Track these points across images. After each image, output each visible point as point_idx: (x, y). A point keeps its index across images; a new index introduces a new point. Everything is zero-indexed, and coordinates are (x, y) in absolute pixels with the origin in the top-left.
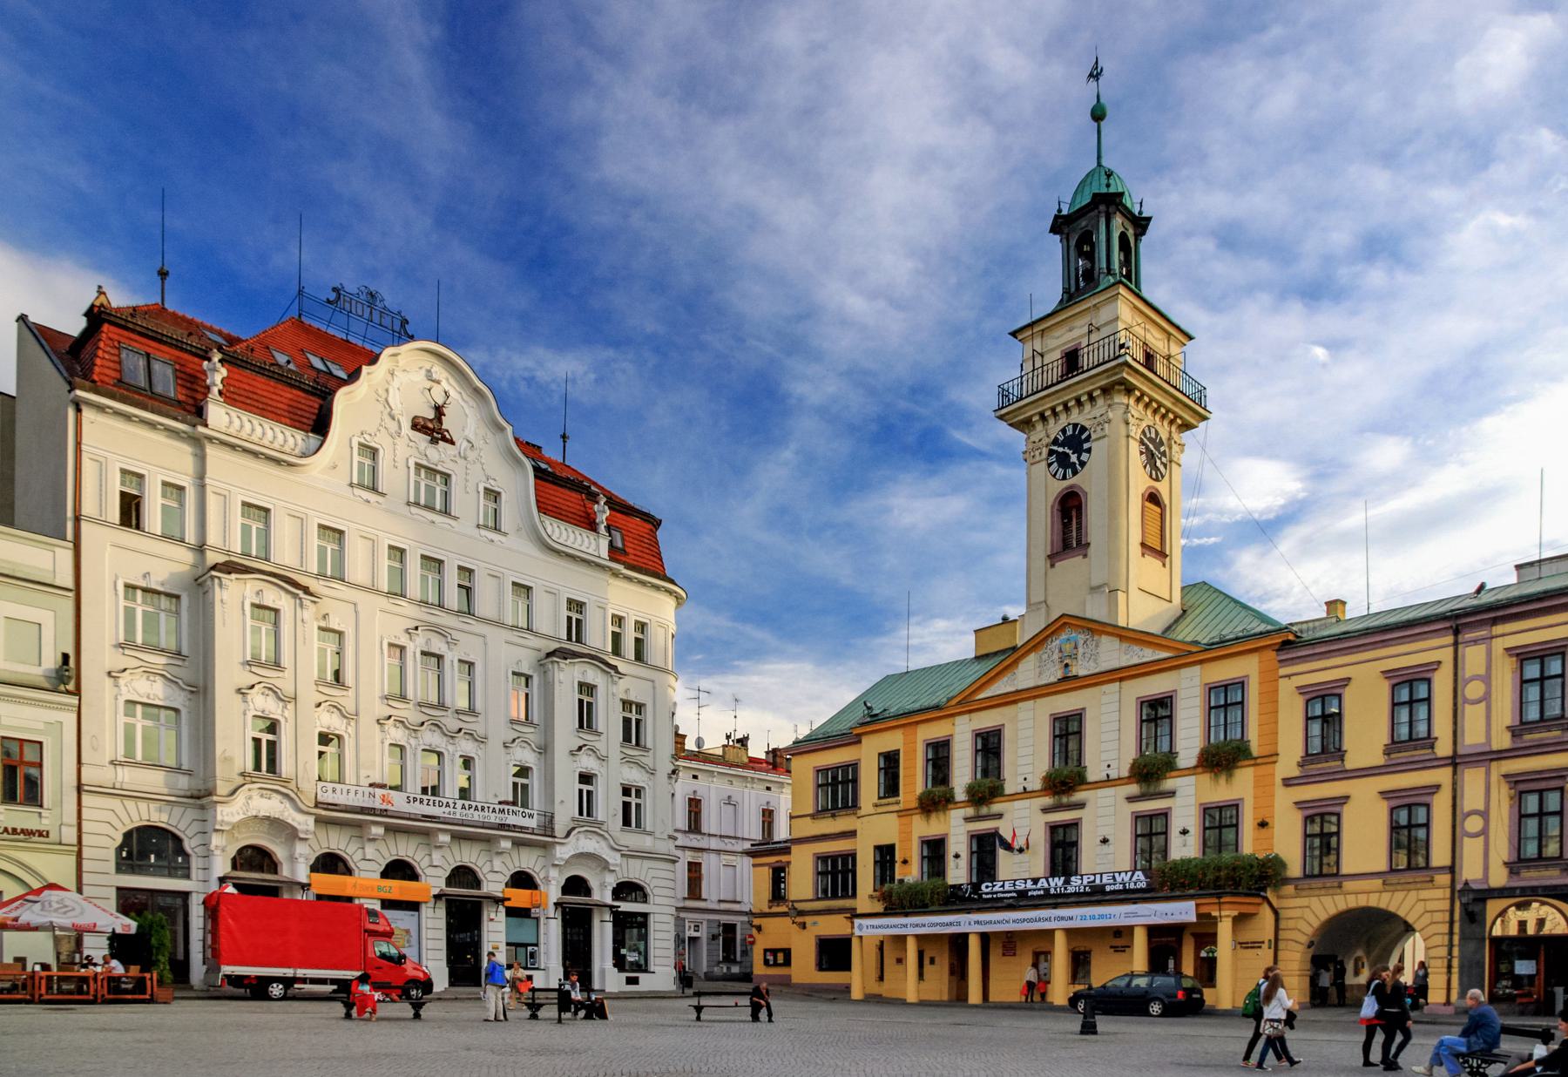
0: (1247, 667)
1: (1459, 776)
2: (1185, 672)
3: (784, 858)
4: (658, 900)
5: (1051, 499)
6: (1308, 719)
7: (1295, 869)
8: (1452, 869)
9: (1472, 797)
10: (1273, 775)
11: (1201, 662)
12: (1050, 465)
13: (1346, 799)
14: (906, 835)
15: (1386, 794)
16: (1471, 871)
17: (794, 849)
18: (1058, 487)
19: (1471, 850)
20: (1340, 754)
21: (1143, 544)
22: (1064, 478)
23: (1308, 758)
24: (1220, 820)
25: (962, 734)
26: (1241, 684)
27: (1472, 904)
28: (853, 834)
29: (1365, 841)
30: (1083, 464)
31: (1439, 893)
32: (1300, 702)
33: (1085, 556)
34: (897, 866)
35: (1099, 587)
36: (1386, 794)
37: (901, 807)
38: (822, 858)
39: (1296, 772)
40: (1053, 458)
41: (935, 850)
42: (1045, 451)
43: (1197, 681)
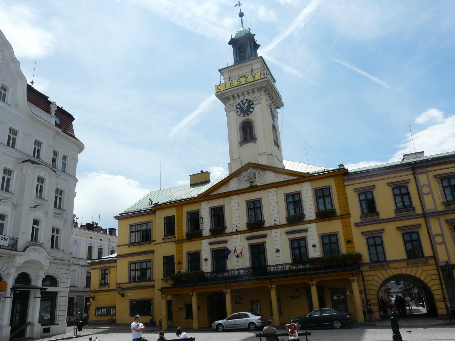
0: (331, 183)
1: (427, 221)
2: (304, 184)
3: (108, 265)
4: (63, 285)
7: (366, 258)
8: (435, 257)
11: (310, 180)
12: (237, 112)
13: (382, 231)
14: (180, 252)
15: (399, 228)
17: (119, 261)
18: (241, 119)
21: (274, 141)
22: (244, 116)
23: (363, 215)
24: (329, 241)
25: (205, 211)
28: (152, 252)
29: (395, 248)
30: (251, 112)
31: (431, 267)
33: (255, 143)
34: (176, 265)
35: (263, 153)
36: (399, 228)
39: (359, 220)
40: (238, 110)
41: (195, 258)
42: (235, 108)
43: (309, 187)
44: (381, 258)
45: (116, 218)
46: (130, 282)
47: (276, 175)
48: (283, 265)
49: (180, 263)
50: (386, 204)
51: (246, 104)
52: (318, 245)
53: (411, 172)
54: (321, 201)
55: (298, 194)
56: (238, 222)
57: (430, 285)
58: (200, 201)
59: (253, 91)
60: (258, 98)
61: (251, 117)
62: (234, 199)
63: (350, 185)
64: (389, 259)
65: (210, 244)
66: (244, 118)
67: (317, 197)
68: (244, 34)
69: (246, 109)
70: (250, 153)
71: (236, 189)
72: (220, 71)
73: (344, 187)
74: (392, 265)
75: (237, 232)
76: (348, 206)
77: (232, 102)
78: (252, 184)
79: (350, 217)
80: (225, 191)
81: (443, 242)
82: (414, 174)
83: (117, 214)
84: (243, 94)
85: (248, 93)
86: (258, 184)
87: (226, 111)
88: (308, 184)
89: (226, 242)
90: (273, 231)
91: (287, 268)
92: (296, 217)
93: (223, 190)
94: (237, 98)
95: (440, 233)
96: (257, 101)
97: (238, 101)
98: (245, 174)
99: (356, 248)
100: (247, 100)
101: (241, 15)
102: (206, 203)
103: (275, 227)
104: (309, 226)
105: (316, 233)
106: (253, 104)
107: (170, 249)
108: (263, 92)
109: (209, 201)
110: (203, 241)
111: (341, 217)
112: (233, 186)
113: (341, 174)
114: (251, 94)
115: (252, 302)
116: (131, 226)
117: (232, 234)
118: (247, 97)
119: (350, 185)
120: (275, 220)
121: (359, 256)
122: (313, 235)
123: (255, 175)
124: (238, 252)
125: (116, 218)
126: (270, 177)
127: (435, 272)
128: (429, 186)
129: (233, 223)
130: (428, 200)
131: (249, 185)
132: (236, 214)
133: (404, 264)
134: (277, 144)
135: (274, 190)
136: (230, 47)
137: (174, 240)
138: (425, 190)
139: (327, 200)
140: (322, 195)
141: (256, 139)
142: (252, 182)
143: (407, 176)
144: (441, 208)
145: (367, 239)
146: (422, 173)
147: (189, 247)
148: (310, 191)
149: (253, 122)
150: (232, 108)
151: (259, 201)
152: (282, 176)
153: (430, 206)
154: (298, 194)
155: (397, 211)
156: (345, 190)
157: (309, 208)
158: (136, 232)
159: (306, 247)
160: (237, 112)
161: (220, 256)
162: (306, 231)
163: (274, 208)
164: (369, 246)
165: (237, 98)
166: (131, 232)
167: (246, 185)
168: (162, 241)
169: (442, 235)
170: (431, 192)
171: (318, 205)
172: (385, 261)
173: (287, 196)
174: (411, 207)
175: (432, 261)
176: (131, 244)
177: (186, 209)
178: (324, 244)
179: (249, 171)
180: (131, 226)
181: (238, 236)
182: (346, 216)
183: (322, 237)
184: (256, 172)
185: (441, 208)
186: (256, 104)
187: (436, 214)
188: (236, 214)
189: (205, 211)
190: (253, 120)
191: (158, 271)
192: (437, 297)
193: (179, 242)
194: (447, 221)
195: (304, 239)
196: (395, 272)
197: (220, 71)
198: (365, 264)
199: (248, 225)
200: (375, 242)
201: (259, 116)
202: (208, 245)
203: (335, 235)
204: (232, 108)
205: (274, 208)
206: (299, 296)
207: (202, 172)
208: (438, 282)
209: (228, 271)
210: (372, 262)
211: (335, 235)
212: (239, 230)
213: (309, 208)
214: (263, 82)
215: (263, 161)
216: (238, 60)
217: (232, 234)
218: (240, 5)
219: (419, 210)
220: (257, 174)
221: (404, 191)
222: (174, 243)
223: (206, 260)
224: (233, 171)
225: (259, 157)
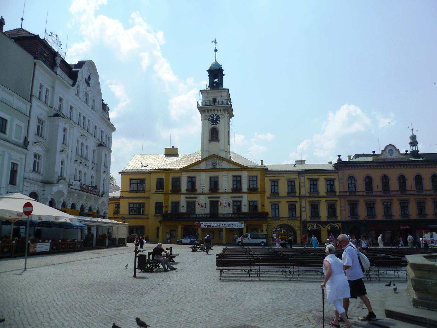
2: (244, 172)
6: (271, 186)
7: (270, 215)
8: (300, 217)
9: (303, 204)
10: (265, 196)
13: (280, 202)
15: (287, 202)
16: (304, 218)
19: (304, 214)
20: (278, 193)
23: (272, 193)
26: (256, 176)
27: (304, 224)
28: (148, 198)
29: (284, 211)
30: (218, 123)
31: (298, 222)
36: (287, 202)
37: (164, 192)
38: (130, 203)
39: (269, 196)
41: (176, 205)
43: (246, 174)
44: (277, 215)
45: (120, 173)
46: (130, 215)
48: (228, 214)
49: (166, 207)
50: (283, 189)
51: (215, 117)
52: (247, 206)
53: (298, 175)
54: (251, 182)
55: (240, 177)
56: (204, 187)
57: (296, 230)
59: (220, 110)
61: (217, 126)
62: (203, 174)
64: (280, 216)
65: (186, 198)
66: (213, 126)
68: (218, 68)
69: (214, 120)
70: (215, 148)
72: (201, 91)
74: (281, 219)
75: (203, 193)
76: (264, 187)
77: (206, 113)
80: (198, 168)
81: (305, 211)
82: (299, 176)
83: (121, 171)
84: (214, 110)
85: (217, 110)
86: (218, 168)
88: (246, 172)
90: (224, 195)
91: (230, 216)
92: (237, 189)
94: (210, 112)
95: (305, 206)
97: (211, 114)
98: (211, 160)
100: (216, 115)
101: (216, 51)
103: (225, 193)
104: (244, 195)
105: (247, 199)
106: (219, 118)
107: (160, 198)
108: (226, 112)
111: (261, 193)
112: (203, 166)
113: (264, 170)
114: (219, 111)
116: (131, 180)
117: (200, 194)
118: (216, 113)
121: (267, 214)
122: (245, 200)
124: (203, 205)
125: (120, 173)
126: (225, 165)
127: (299, 224)
128: (304, 183)
129: (201, 188)
130: (303, 190)
131: (212, 167)
132: (203, 182)
133: (287, 219)
134: (229, 144)
136: (207, 74)
137: (163, 193)
138: (302, 185)
139: (255, 182)
140: (252, 179)
143: (295, 176)
144: (307, 194)
145: (272, 205)
146: (302, 176)
147: (173, 198)
152: (232, 165)
153: (303, 193)
154: (240, 177)
155: (288, 193)
156: (264, 179)
157: (245, 186)
158: (134, 184)
161: (191, 205)
162: (242, 197)
163: (225, 182)
164: (272, 209)
165: (210, 112)
166: (131, 184)
167: (210, 167)
168: (154, 192)
169: (305, 207)
170: (305, 186)
171: (249, 184)
172: (279, 217)
173: (233, 177)
174: (295, 192)
175: (299, 219)
176: (130, 191)
177: (172, 175)
178: (250, 206)
179: (213, 159)
180: (131, 180)
182: (263, 192)
183: (250, 201)
184: (218, 160)
185: (307, 194)
187: (305, 197)
188: (203, 182)
190: (219, 128)
191: (151, 209)
192: (298, 235)
193: (166, 194)
194: (309, 201)
195: (240, 202)
196: (282, 223)
197: (201, 91)
199: (210, 190)
200: (275, 206)
201: (221, 126)
202: (185, 198)
203: (257, 201)
205: (225, 182)
207: (173, 147)
208: (300, 228)
209: (196, 214)
210: (272, 217)
211: (257, 201)
212: (204, 192)
213: (245, 186)
215: (222, 155)
217: (200, 194)
218: (216, 43)
219: (298, 195)
220: (217, 162)
221: (293, 184)
222: (163, 195)
223: (183, 207)
224: (204, 157)
225: (220, 152)
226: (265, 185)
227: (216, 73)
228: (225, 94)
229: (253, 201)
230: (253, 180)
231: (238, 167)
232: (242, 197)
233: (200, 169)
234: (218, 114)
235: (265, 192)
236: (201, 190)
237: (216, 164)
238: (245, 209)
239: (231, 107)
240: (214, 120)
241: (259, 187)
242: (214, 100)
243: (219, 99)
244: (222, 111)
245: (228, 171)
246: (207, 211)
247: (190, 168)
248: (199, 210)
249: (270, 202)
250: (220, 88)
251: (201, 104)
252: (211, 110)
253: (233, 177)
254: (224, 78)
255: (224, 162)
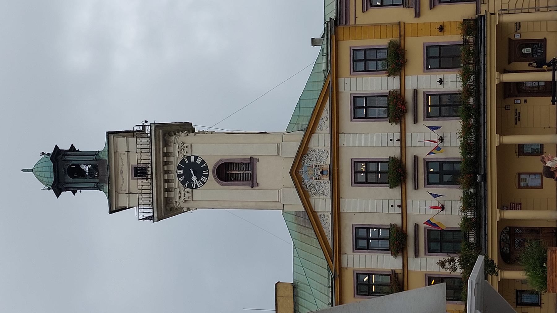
5: (218, 185)
11: (337, 77)
30: (203, 162)
32: (373, 11)
33: (257, 160)
39: (412, 11)
47: (318, 131)
52: (440, 76)
55: (355, 98)
58: (340, 268)
60: (181, 148)
61: (211, 164)
63: (356, 18)
65: (417, 255)
67: (366, 70)
71: (329, 201)
72: (111, 212)
73: (356, 26)
76: (387, 25)
77: (175, 195)
78: (325, 173)
79: (404, 23)
80: (329, 221)
84: (166, 172)
86: (328, 162)
87: (189, 209)
89: (417, 226)
90: (408, 144)
93: (327, 224)
94: (172, 185)
96: (186, 149)
97: (177, 183)
98: (307, 182)
99: (452, 20)
100: (179, 168)
102: (344, 257)
103: (402, 140)
106: (189, 158)
108: (173, 138)
109: (342, 251)
110: (411, 268)
111: (402, 36)
112: (323, 205)
115: (520, 187)
119: (356, 18)
120: (391, 140)
123: (312, 167)
126: (321, 141)
132: (372, 205)
135: (341, 136)
136: (66, 195)
140: (363, 61)
141: (252, 158)
142: (322, 173)
148: (354, 79)
149: (221, 160)
150: (187, 195)
151: (355, 163)
154: (355, 98)
156: (362, 26)
157: (381, 84)
159: (440, 95)
160: (197, 187)
162: (416, 92)
163: (372, 140)
165: (172, 185)
167: (326, 184)
179: (303, 176)
181: (409, 203)
183: (428, 67)
184: (307, 163)
186: (191, 152)
188: (372, 205)
189: (357, 261)
197: (111, 212)
198: (478, 10)
201: (211, 154)
202: (417, 260)
203: (428, 48)
204: (187, 195)
205: (372, 140)
206: (516, 110)
211: (428, 48)
213: (381, 84)
214: (155, 134)
216: (97, 180)
217: (404, 215)
226: (380, 25)
227: (68, 170)
228: (122, 142)
229: (428, 58)
230: (366, 60)
231: (328, 103)
232: (416, 92)
233: (333, 213)
234: (176, 161)
235: (399, 23)
236: (392, 210)
237: (317, 167)
238: (453, 82)
239: (158, 126)
240: (193, 170)
241: (384, 42)
242: (140, 172)
243: (134, 162)
244: (171, 150)
245: (338, 133)
246: (454, 196)
247: (330, 242)
248: (453, 218)
249: (432, 6)
250: (106, 158)
251: (148, 211)
252: (166, 181)
253: (355, 117)
254: (82, 147)
255: (311, 145)
